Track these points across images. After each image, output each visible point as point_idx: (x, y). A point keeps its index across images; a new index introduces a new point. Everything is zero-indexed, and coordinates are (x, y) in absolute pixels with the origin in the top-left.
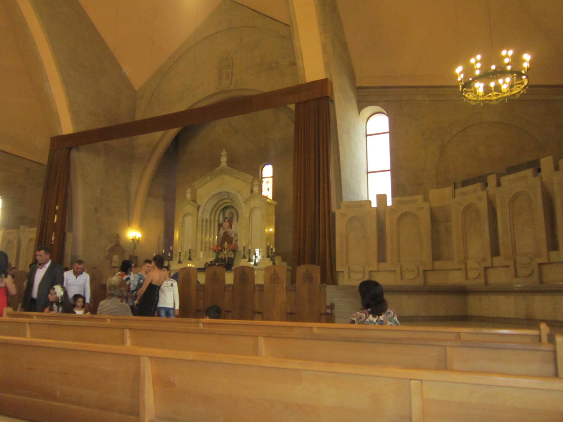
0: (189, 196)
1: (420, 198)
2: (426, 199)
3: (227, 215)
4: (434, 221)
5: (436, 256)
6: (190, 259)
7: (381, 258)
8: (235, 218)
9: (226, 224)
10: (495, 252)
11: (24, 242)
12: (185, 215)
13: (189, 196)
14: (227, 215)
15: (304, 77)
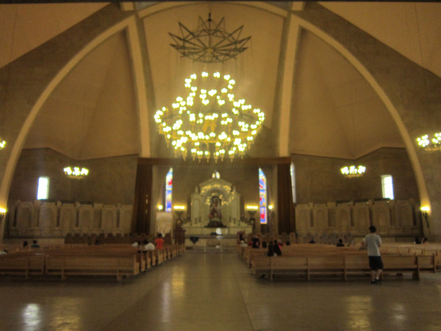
0: (197, 190)
1: (324, 205)
2: (327, 206)
3: (215, 200)
4: (329, 213)
5: (330, 225)
6: (200, 221)
7: (312, 225)
8: (219, 202)
9: (214, 205)
10: (352, 224)
11: (122, 212)
12: (194, 200)
13: (197, 190)
14: (215, 200)
15: (279, 154)
